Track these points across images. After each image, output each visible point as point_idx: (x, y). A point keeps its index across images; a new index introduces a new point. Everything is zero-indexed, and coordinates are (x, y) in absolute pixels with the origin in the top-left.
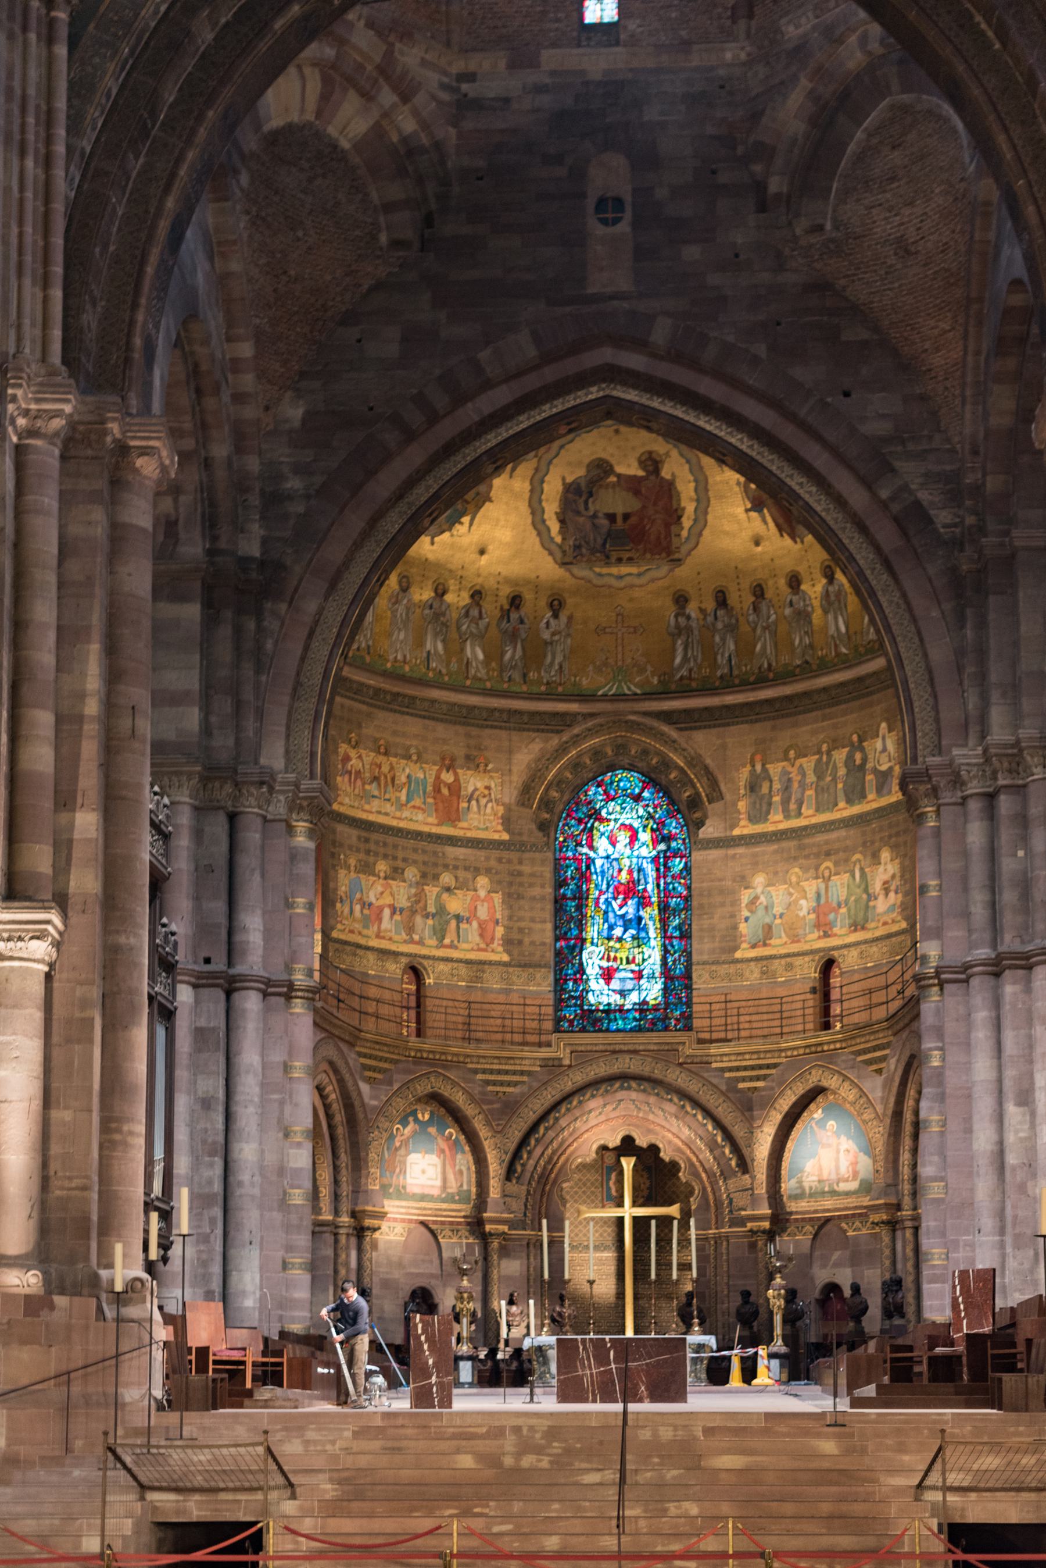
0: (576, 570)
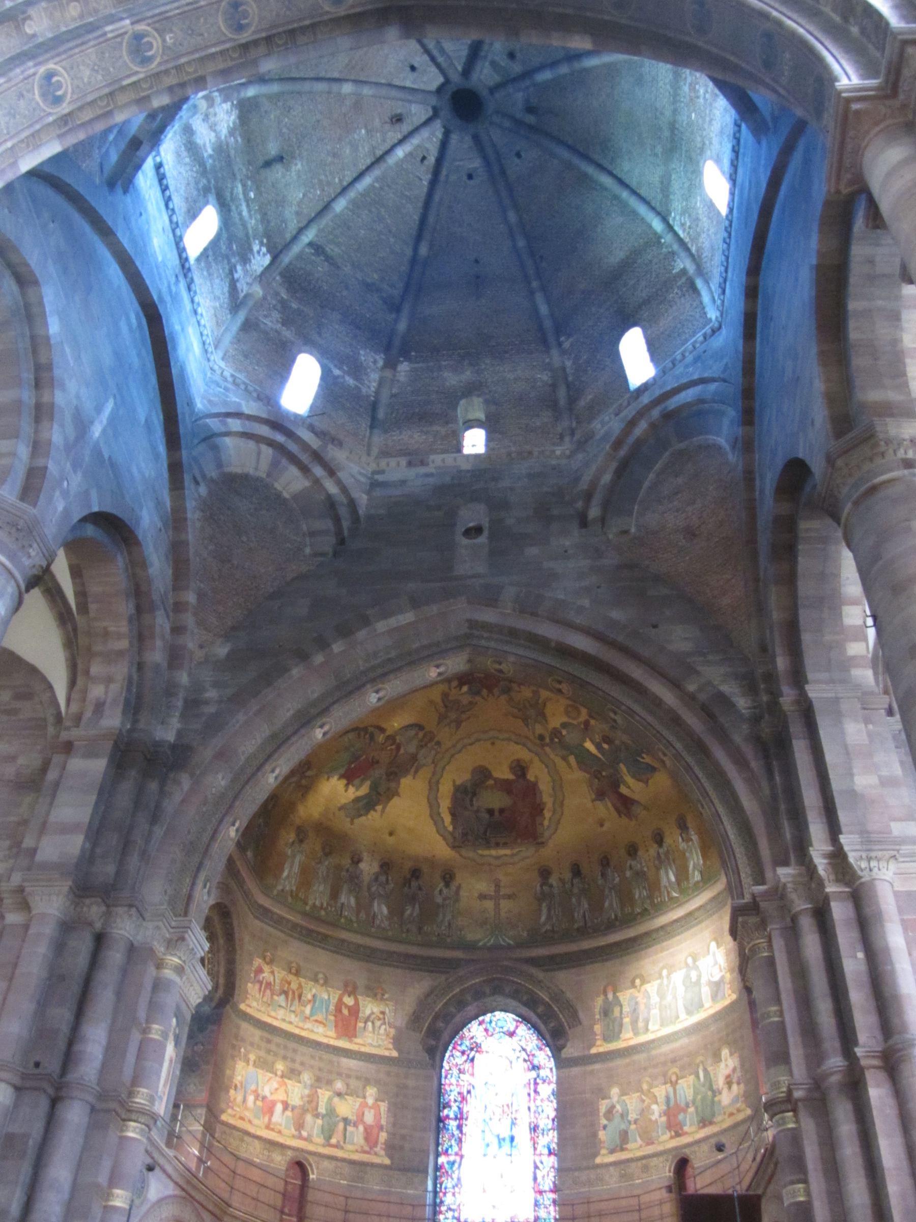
0: (464, 852)
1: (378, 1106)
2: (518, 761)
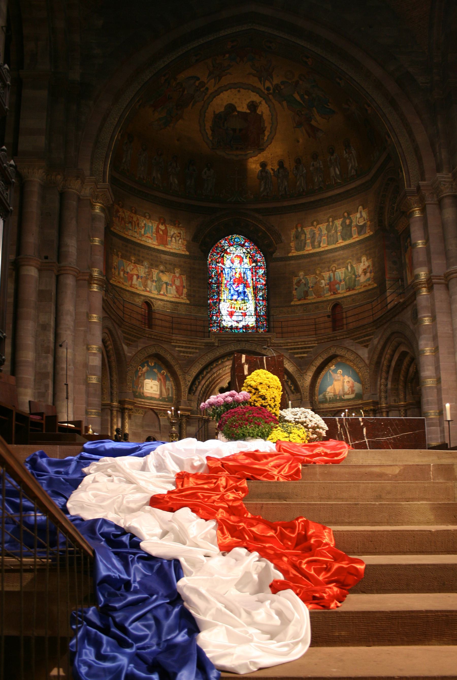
1: (181, 277)
2: (253, 102)
